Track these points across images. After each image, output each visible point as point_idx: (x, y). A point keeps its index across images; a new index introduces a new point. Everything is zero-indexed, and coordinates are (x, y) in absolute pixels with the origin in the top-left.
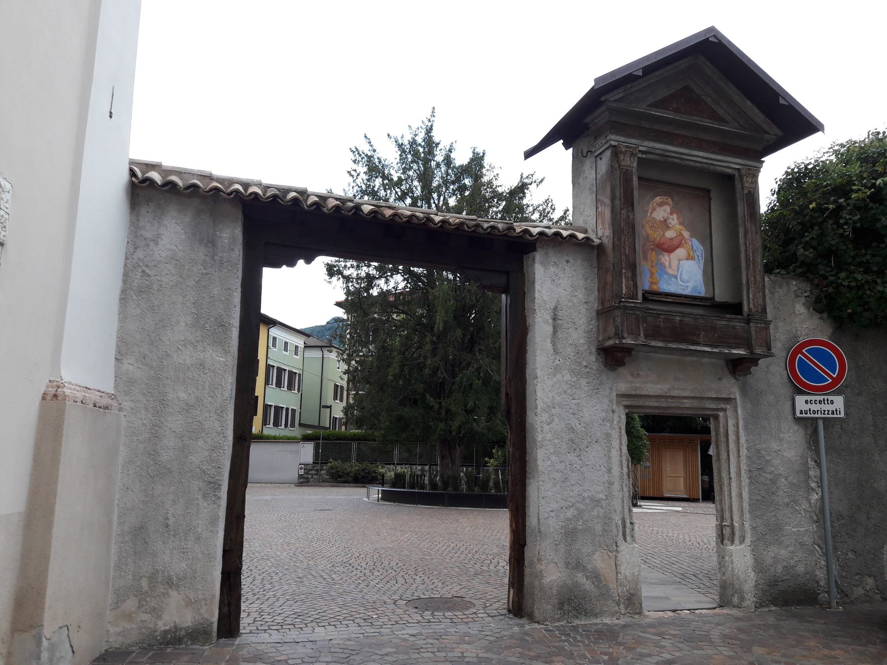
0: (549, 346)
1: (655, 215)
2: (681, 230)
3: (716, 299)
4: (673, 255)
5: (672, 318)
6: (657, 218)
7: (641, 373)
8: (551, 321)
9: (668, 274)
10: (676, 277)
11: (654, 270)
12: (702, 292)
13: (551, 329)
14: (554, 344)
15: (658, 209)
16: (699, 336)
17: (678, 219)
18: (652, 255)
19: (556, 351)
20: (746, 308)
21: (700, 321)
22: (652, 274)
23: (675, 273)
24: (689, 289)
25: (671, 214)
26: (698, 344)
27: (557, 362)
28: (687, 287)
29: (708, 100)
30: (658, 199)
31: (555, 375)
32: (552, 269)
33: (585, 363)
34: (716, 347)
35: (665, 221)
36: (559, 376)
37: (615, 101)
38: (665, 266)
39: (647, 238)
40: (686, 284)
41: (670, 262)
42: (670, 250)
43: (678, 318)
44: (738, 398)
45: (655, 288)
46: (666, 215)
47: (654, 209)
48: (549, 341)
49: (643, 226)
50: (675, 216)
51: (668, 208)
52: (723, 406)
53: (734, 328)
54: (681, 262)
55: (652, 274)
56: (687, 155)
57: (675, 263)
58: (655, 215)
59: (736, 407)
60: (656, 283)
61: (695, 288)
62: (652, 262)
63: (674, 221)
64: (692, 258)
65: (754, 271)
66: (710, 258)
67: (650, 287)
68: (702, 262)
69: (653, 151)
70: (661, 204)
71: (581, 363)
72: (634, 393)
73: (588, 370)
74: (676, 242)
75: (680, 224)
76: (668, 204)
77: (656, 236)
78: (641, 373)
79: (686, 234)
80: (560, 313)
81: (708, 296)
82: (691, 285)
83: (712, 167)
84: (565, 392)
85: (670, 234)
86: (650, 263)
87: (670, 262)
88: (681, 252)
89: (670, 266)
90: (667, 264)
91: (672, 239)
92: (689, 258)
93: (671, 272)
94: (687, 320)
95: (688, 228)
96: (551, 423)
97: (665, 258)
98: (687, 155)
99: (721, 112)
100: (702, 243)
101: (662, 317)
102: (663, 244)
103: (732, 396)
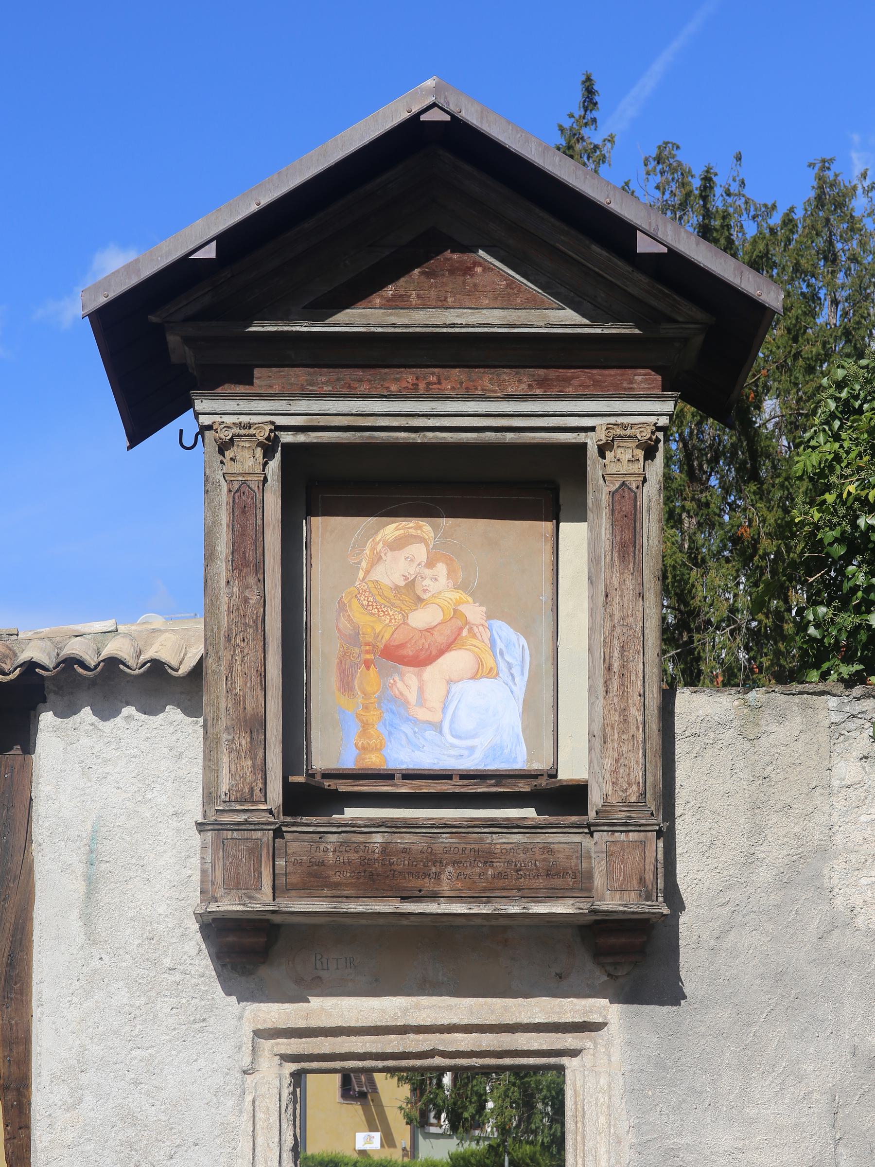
0: (75, 925)
2: (459, 602)
4: (430, 672)
5: (361, 838)
6: (385, 581)
7: (324, 974)
8: (80, 869)
9: (415, 721)
10: (437, 727)
13: (80, 886)
14: (88, 920)
16: (437, 876)
18: (368, 680)
19: (92, 937)
20: (595, 799)
21: (446, 840)
22: (365, 726)
23: (436, 718)
25: (430, 564)
26: (434, 897)
27: (95, 964)
28: (472, 749)
32: (85, 741)
33: (167, 962)
34: (489, 900)
35: (411, 584)
37: (187, 320)
38: (407, 702)
39: (355, 637)
40: (469, 743)
41: (421, 690)
43: (378, 838)
45: (373, 761)
46: (412, 570)
47: (377, 559)
48: (74, 915)
49: (342, 607)
50: (441, 569)
51: (419, 552)
52: (569, 1041)
53: (547, 849)
54: (455, 688)
55: (365, 726)
57: (434, 694)
59: (609, 1044)
60: (378, 749)
62: (366, 695)
63: (438, 582)
64: (492, 673)
65: (624, 696)
66: (548, 667)
68: (521, 682)
70: (398, 544)
71: (156, 962)
73: (178, 977)
74: (440, 638)
75: (457, 587)
77: (382, 628)
78: (324, 974)
79: (474, 612)
81: (536, 766)
85: (421, 619)
87: (421, 690)
88: (455, 661)
89: (421, 700)
90: (412, 697)
93: (422, 714)
94: (405, 840)
96: (73, 1107)
97: (407, 683)
100: (526, 631)
101: (333, 838)
102: (402, 646)
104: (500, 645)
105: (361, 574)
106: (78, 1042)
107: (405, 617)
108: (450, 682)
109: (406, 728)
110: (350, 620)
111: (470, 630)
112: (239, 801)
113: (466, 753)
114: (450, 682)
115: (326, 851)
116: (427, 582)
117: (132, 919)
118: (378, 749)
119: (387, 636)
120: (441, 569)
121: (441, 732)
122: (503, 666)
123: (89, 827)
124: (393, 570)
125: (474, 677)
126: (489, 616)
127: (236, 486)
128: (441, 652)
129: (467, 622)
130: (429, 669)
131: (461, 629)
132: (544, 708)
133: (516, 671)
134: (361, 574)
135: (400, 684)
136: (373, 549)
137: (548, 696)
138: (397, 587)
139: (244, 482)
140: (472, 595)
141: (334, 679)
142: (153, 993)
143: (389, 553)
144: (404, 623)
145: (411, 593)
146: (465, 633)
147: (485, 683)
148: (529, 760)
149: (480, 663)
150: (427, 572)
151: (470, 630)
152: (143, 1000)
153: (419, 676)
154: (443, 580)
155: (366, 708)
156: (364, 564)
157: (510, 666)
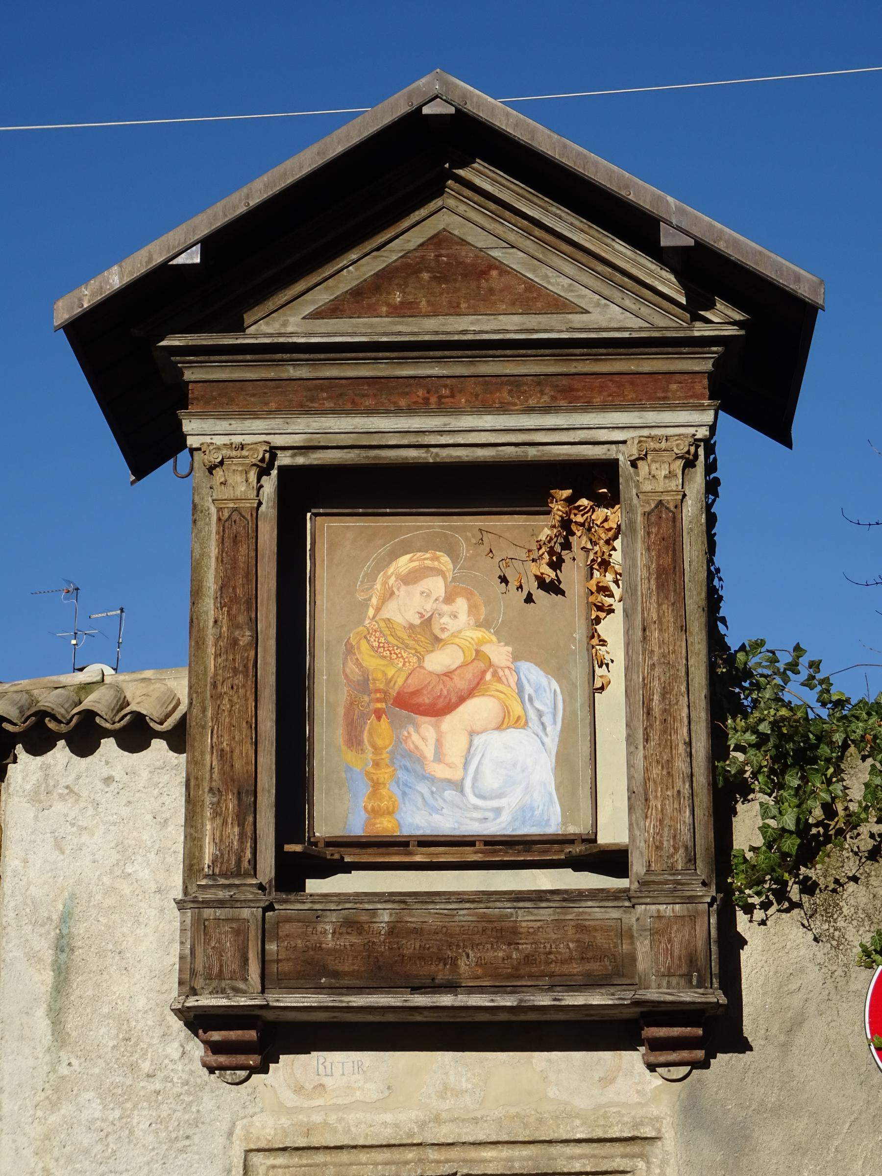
0: (41, 1024)
1: (391, 611)
2: (481, 642)
3: (602, 840)
4: (449, 722)
6: (399, 619)
8: (48, 955)
10: (459, 786)
11: (383, 774)
12: (550, 819)
13: (48, 976)
14: (56, 1016)
15: (402, 592)
17: (470, 613)
20: (637, 866)
22: (376, 785)
23: (457, 775)
24: (505, 817)
25: (449, 599)
26: (451, 987)
28: (498, 811)
29: (514, 260)
30: (404, 563)
31: (54, 1106)
33: (146, 1066)
34: (514, 990)
35: (427, 622)
36: (66, 1109)
38: (421, 760)
39: (364, 684)
40: (495, 803)
41: (439, 743)
42: (439, 709)
44: (669, 1135)
45: (385, 827)
46: (429, 606)
48: (41, 1012)
49: (350, 650)
50: (461, 604)
51: (437, 586)
54: (478, 741)
55: (376, 785)
56: (441, 433)
57: (455, 747)
58: (391, 611)
60: (390, 813)
61: (525, 811)
63: (459, 620)
64: (521, 723)
67: (368, 824)
69: (323, 441)
70: (410, 578)
71: (133, 1067)
72: (301, 1142)
74: (460, 684)
75: (479, 625)
76: (440, 572)
77: (394, 673)
79: (499, 654)
80: (79, 929)
81: (572, 829)
82: (510, 803)
83: (532, 453)
84: (86, 1152)
85: (439, 661)
86: (369, 754)
87: (439, 743)
88: (479, 709)
89: (439, 757)
90: (429, 752)
91: (448, 674)
92: (507, 721)
93: (440, 771)
95: (505, 634)
97: (423, 735)
98: (441, 433)
99: (557, 284)
100: (559, 673)
102: (417, 693)
103: (647, 1131)
104: (528, 690)
105: (371, 612)
106: (41, 1165)
107: (421, 659)
108: (472, 734)
109: (423, 788)
110: (358, 664)
111: (495, 674)
112: (223, 875)
113: (491, 815)
114: (472, 734)
115: (325, 932)
116: (445, 620)
117: (107, 1016)
118: (390, 813)
119: (400, 682)
120: (461, 604)
121: (462, 791)
122: (532, 714)
123: (61, 907)
124: (406, 607)
125: (500, 727)
126: (516, 657)
127: (226, 514)
128: (462, 700)
129: (490, 664)
130: (448, 718)
131: (484, 673)
132: (578, 764)
133: (547, 719)
134: (371, 612)
135: (415, 737)
136: (385, 583)
137: (584, 748)
138: (411, 626)
139: (235, 510)
140: (496, 633)
141: (339, 734)
142: (129, 1105)
143: (403, 588)
144: (420, 667)
145: (427, 633)
146: (488, 676)
147: (513, 735)
148: (564, 823)
149: (506, 711)
150: (446, 608)
151: (495, 674)
152: (117, 1113)
153: (437, 727)
154: (463, 617)
155: (376, 764)
156: (374, 601)
157: (540, 714)
